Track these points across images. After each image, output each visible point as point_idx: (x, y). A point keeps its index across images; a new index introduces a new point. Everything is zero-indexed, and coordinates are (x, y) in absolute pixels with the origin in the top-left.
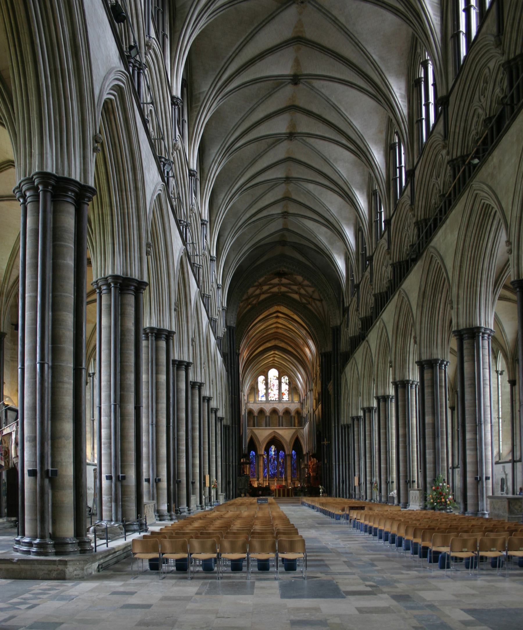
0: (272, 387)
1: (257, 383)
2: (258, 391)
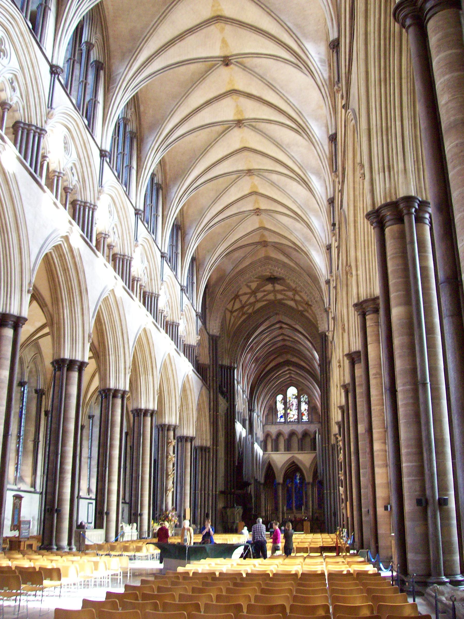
0: (291, 407)
1: (276, 403)
2: (276, 411)
